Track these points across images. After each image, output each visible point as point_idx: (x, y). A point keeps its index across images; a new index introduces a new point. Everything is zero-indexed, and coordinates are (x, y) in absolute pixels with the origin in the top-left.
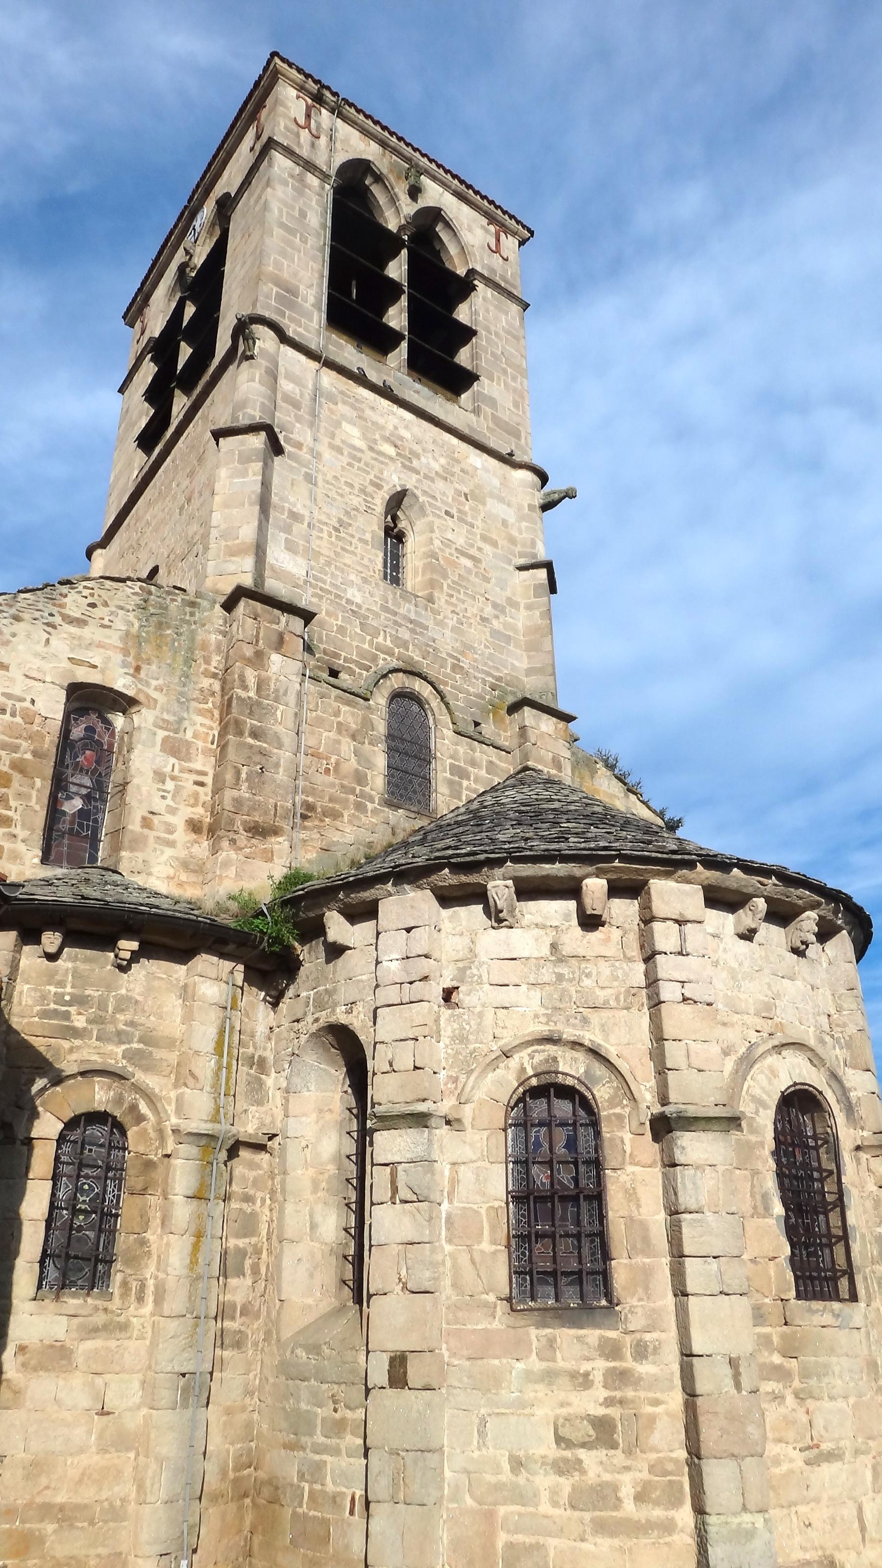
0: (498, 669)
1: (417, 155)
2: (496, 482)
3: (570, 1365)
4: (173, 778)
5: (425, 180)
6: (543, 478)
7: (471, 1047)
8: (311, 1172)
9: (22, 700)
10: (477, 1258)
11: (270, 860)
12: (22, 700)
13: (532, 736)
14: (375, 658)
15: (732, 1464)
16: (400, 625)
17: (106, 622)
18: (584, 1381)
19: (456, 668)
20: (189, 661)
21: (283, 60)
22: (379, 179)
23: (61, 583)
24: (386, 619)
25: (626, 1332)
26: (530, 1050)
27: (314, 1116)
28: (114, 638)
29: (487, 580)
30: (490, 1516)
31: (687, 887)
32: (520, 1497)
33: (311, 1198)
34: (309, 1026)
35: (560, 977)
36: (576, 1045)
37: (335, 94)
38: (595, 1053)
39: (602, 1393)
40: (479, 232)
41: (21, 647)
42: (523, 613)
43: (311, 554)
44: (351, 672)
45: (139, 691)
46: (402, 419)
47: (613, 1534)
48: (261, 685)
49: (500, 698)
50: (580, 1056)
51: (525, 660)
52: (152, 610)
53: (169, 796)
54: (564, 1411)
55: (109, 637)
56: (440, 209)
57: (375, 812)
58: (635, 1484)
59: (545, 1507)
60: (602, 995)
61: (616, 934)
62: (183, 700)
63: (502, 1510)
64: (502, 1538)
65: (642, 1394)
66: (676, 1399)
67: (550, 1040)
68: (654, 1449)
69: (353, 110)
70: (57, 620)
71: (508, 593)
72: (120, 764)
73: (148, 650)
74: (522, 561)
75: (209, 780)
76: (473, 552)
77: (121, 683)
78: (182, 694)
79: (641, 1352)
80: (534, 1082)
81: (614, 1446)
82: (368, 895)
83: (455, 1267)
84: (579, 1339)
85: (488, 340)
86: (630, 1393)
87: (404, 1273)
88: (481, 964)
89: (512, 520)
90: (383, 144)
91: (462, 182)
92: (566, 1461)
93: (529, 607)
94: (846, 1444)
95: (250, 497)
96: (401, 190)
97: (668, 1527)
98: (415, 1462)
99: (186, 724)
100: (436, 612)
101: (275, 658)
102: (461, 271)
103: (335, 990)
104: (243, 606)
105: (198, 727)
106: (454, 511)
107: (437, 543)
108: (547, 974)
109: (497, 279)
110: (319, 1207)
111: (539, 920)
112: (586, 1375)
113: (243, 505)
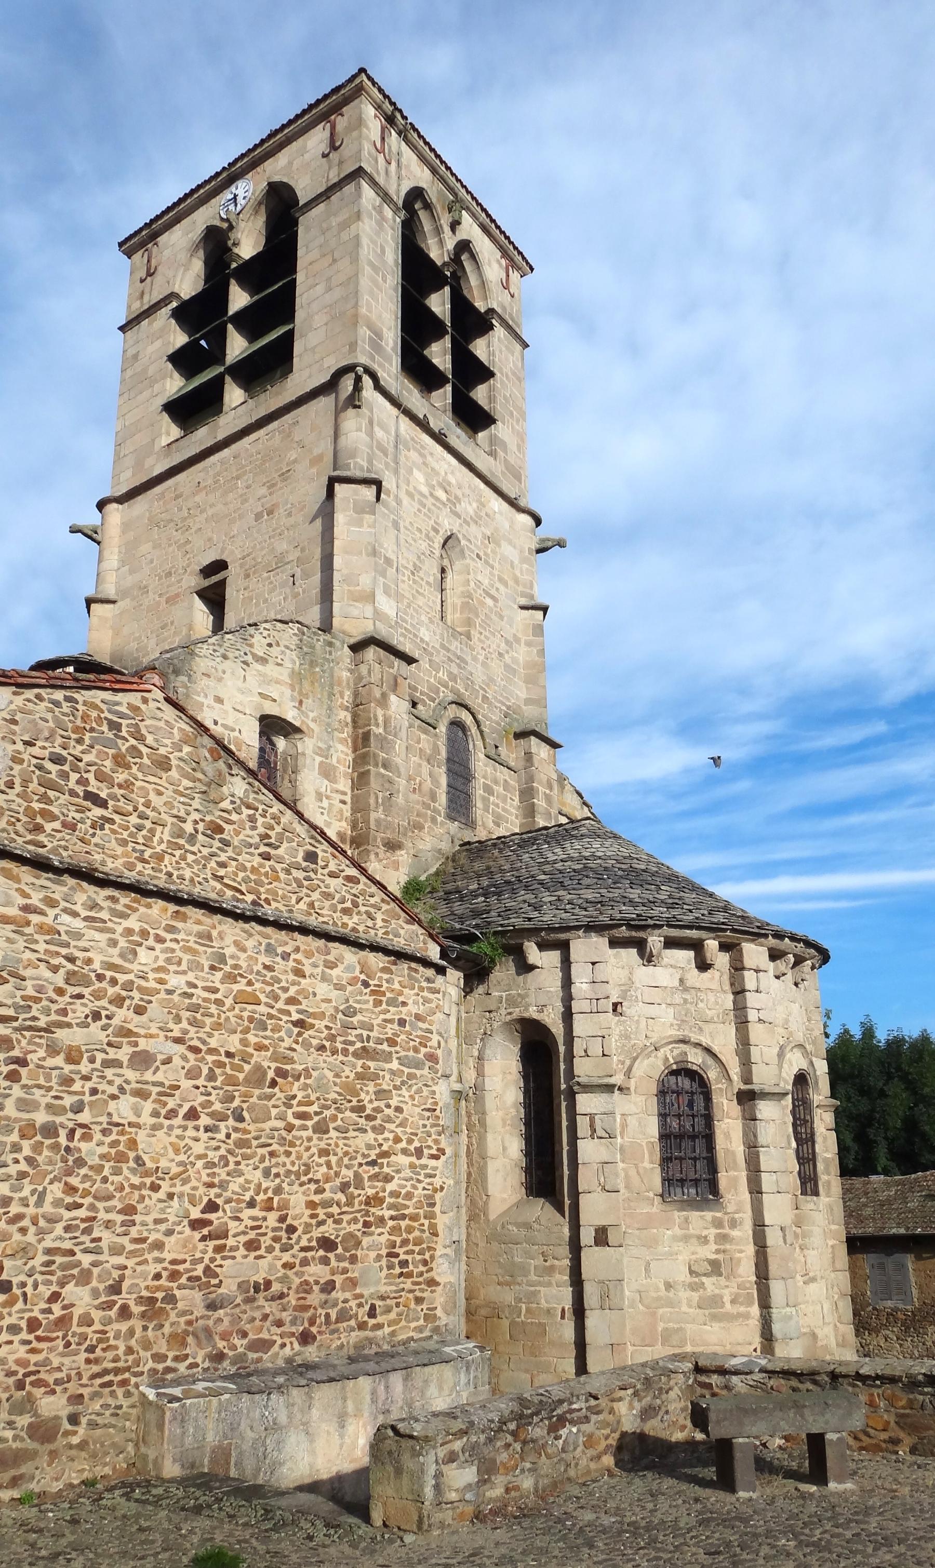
0: (508, 699)
1: (459, 185)
2: (507, 525)
3: (697, 1232)
4: (328, 797)
5: (465, 216)
6: (538, 521)
7: (633, 1042)
8: (501, 1113)
9: (233, 730)
10: (641, 1171)
11: (397, 869)
12: (233, 730)
13: (536, 759)
14: (437, 692)
15: (781, 1282)
16: (452, 661)
17: (279, 661)
18: (704, 1240)
19: (485, 698)
20: (331, 695)
21: (369, 78)
22: (428, 206)
23: (250, 625)
24: (444, 656)
25: (726, 1213)
26: (671, 1046)
27: (500, 1076)
28: (283, 674)
29: (501, 618)
30: (654, 1314)
31: (761, 949)
32: (670, 1304)
33: (502, 1130)
34: (502, 1016)
35: (685, 1001)
36: (698, 1045)
37: (405, 118)
38: (708, 1050)
39: (714, 1247)
40: (495, 266)
41: (229, 683)
42: (523, 649)
43: (399, 597)
44: (425, 705)
45: (303, 722)
46: (450, 465)
47: (720, 1321)
48: (387, 721)
49: (510, 725)
50: (698, 1051)
51: (524, 690)
52: (305, 649)
53: (325, 812)
54: (694, 1257)
55: (281, 674)
56: (470, 242)
57: (442, 823)
58: (731, 1294)
59: (685, 1308)
60: (710, 1013)
61: (717, 974)
62: (329, 730)
63: (661, 1311)
64: (661, 1326)
65: (734, 1247)
66: (750, 1249)
67: (683, 1041)
68: (740, 1276)
69: (415, 135)
70: (249, 658)
71: (514, 631)
72: (286, 782)
73: (306, 685)
74: (523, 601)
75: (348, 798)
76: (493, 592)
77: (291, 715)
78: (328, 725)
79: (734, 1224)
80: (674, 1067)
81: (721, 1275)
82: (563, 936)
83: (627, 1176)
84: (701, 1217)
85: (502, 382)
86: (728, 1247)
87: (602, 1180)
88: (637, 989)
89: (516, 562)
90: (434, 171)
91: (488, 215)
92: (696, 1283)
93: (528, 644)
94: (818, 1273)
95: (366, 549)
96: (445, 220)
97: (747, 1316)
98: (616, 1287)
99: (332, 751)
100: (473, 649)
101: (393, 698)
102: (481, 306)
103: (527, 995)
104: (371, 653)
105: (339, 754)
106: (481, 554)
107: (472, 584)
108: (678, 998)
109: (507, 317)
110: (507, 1137)
111: (673, 962)
112: (706, 1237)
113: (361, 553)
